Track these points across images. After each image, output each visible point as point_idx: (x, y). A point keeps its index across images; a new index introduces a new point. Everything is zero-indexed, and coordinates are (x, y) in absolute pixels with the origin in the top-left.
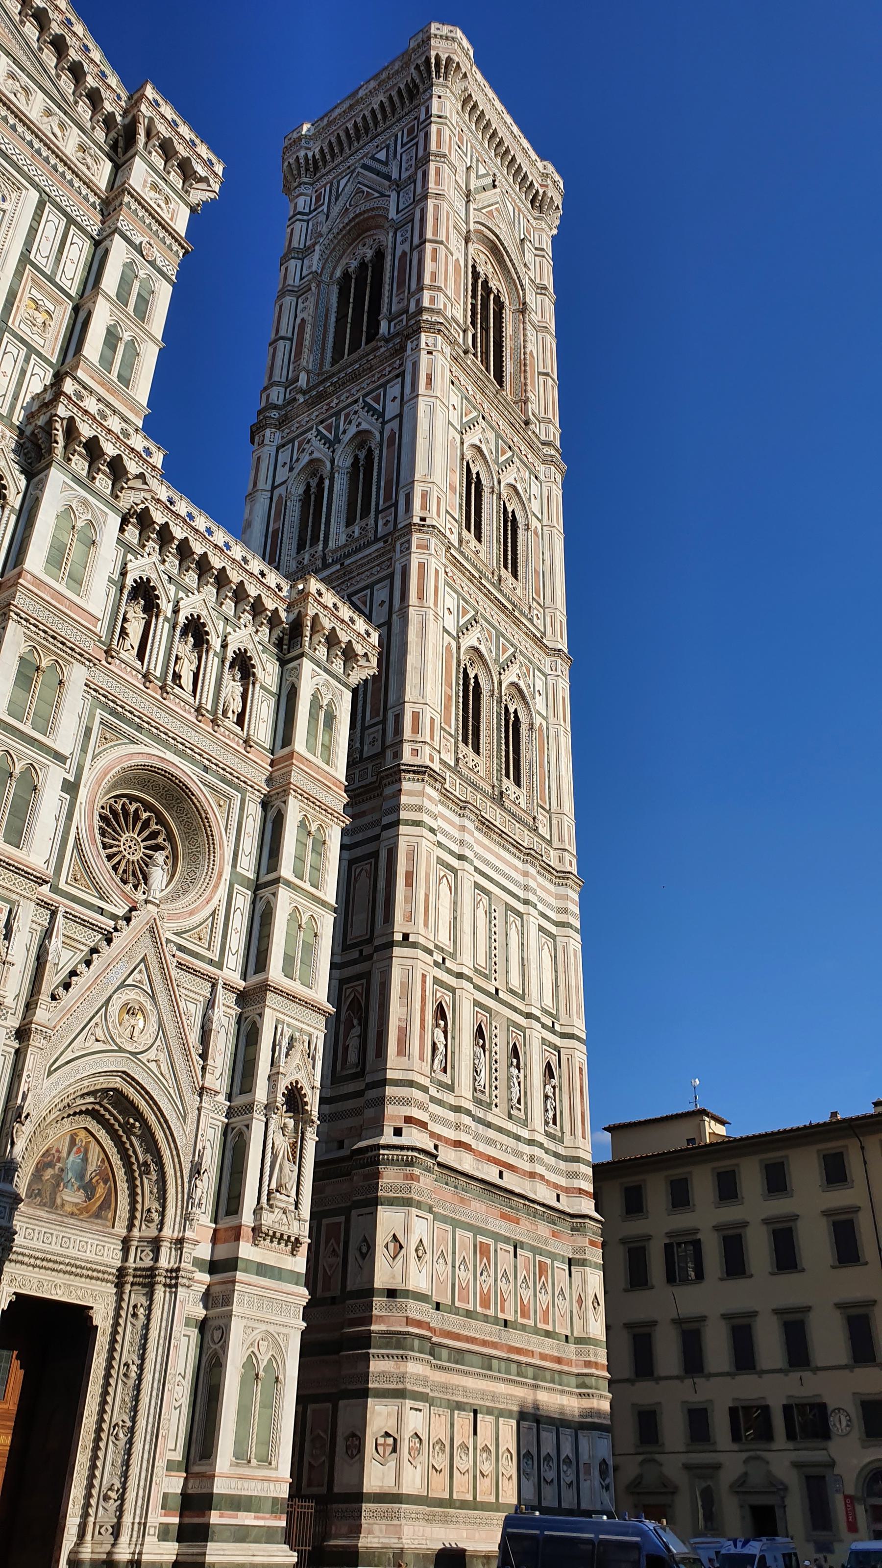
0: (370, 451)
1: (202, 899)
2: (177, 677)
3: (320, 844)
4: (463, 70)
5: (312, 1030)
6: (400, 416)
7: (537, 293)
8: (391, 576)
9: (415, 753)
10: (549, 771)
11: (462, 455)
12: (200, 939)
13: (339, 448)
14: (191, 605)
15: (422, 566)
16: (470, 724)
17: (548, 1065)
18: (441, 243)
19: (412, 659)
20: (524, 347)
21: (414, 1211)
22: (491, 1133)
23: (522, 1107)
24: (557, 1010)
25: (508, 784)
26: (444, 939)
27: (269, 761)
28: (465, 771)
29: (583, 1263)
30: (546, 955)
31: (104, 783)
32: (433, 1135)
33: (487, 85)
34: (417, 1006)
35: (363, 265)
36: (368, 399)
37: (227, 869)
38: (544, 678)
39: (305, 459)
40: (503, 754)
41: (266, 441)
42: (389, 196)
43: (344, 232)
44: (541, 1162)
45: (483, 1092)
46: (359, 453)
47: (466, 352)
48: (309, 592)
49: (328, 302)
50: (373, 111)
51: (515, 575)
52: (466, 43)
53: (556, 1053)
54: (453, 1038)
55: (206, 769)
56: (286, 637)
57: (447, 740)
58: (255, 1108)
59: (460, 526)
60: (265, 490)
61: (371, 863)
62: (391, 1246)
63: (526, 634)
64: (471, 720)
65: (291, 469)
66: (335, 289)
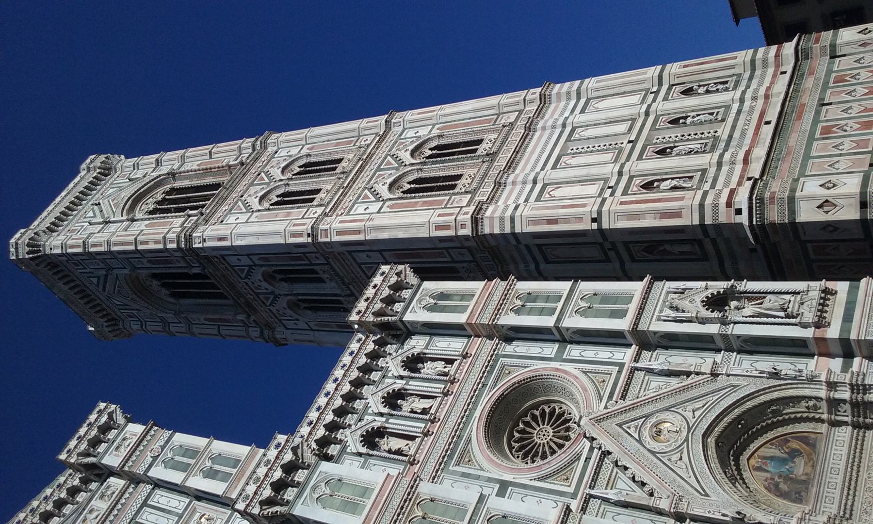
0: (275, 272)
1: (575, 383)
2: (425, 411)
3: (531, 297)
4: (33, 235)
5: (664, 291)
6: (248, 255)
8: (350, 252)
9: (463, 226)
10: (470, 119)
12: (604, 381)
13: (277, 292)
16: (442, 184)
17: (683, 93)
19: (401, 235)
20: (195, 171)
21: (798, 194)
22: (737, 134)
23: (716, 111)
24: (642, 90)
25: (482, 149)
26: (593, 189)
27: (476, 338)
28: (474, 186)
29: (833, 46)
31: (499, 462)
32: (740, 184)
33: (40, 217)
34: (643, 206)
35: (164, 285)
36: (243, 276)
38: (407, 130)
39: (289, 312)
40: (460, 156)
42: (117, 274)
43: (146, 299)
44: (756, 91)
45: (706, 144)
46: (278, 278)
47: (202, 214)
48: (359, 321)
51: (339, 161)
52: (17, 236)
53: (674, 87)
54: (666, 173)
55: (484, 385)
56: (391, 333)
57: (453, 201)
58: (724, 333)
59: (311, 206)
60: (314, 335)
61: (546, 249)
62: (826, 209)
63: (378, 148)
64: (439, 184)
65: (298, 320)
66: (182, 301)
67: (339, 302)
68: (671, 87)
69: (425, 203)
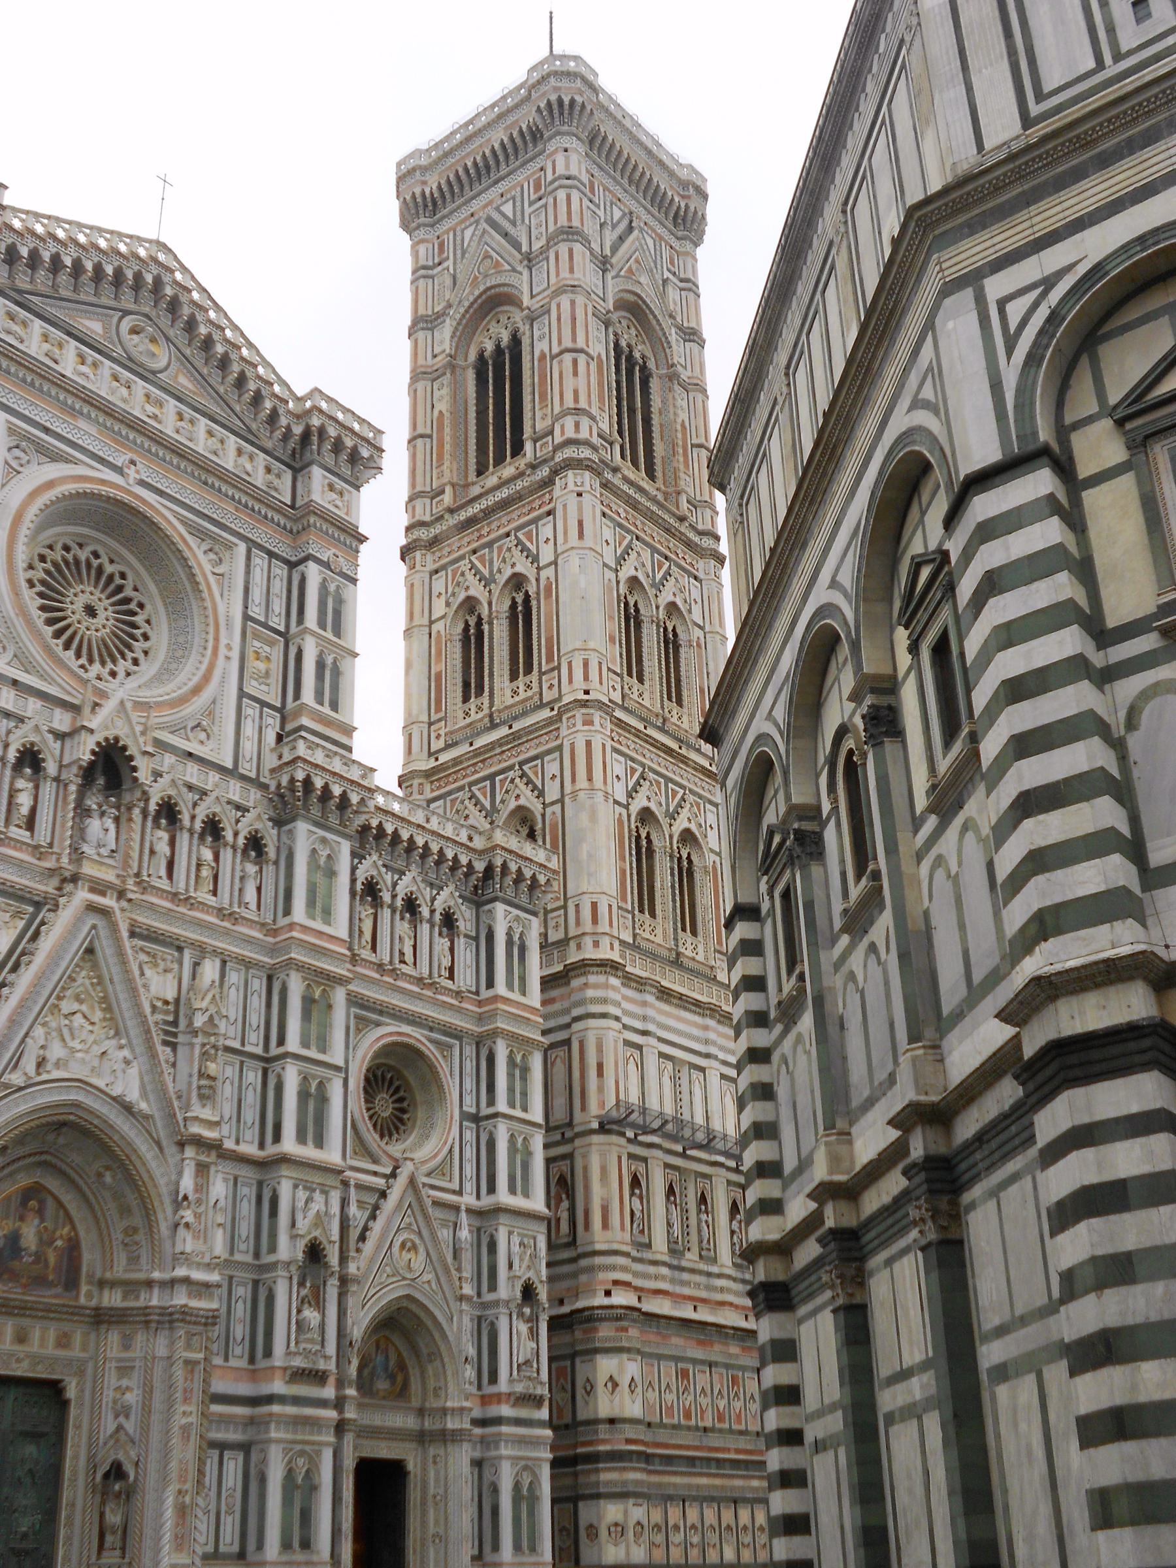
0: (527, 595)
3: (525, 1070)
6: (555, 563)
7: (685, 341)
8: (560, 748)
9: (596, 944)
11: (618, 596)
14: (405, 885)
15: (588, 744)
22: (686, 1276)
25: (686, 937)
28: (643, 944)
34: (616, 1185)
35: (499, 350)
36: (519, 534)
41: (418, 567)
50: (493, 151)
54: (648, 1202)
55: (431, 1029)
62: (610, 1385)
63: (695, 769)
65: (448, 604)
66: (471, 375)
69: (623, 872)
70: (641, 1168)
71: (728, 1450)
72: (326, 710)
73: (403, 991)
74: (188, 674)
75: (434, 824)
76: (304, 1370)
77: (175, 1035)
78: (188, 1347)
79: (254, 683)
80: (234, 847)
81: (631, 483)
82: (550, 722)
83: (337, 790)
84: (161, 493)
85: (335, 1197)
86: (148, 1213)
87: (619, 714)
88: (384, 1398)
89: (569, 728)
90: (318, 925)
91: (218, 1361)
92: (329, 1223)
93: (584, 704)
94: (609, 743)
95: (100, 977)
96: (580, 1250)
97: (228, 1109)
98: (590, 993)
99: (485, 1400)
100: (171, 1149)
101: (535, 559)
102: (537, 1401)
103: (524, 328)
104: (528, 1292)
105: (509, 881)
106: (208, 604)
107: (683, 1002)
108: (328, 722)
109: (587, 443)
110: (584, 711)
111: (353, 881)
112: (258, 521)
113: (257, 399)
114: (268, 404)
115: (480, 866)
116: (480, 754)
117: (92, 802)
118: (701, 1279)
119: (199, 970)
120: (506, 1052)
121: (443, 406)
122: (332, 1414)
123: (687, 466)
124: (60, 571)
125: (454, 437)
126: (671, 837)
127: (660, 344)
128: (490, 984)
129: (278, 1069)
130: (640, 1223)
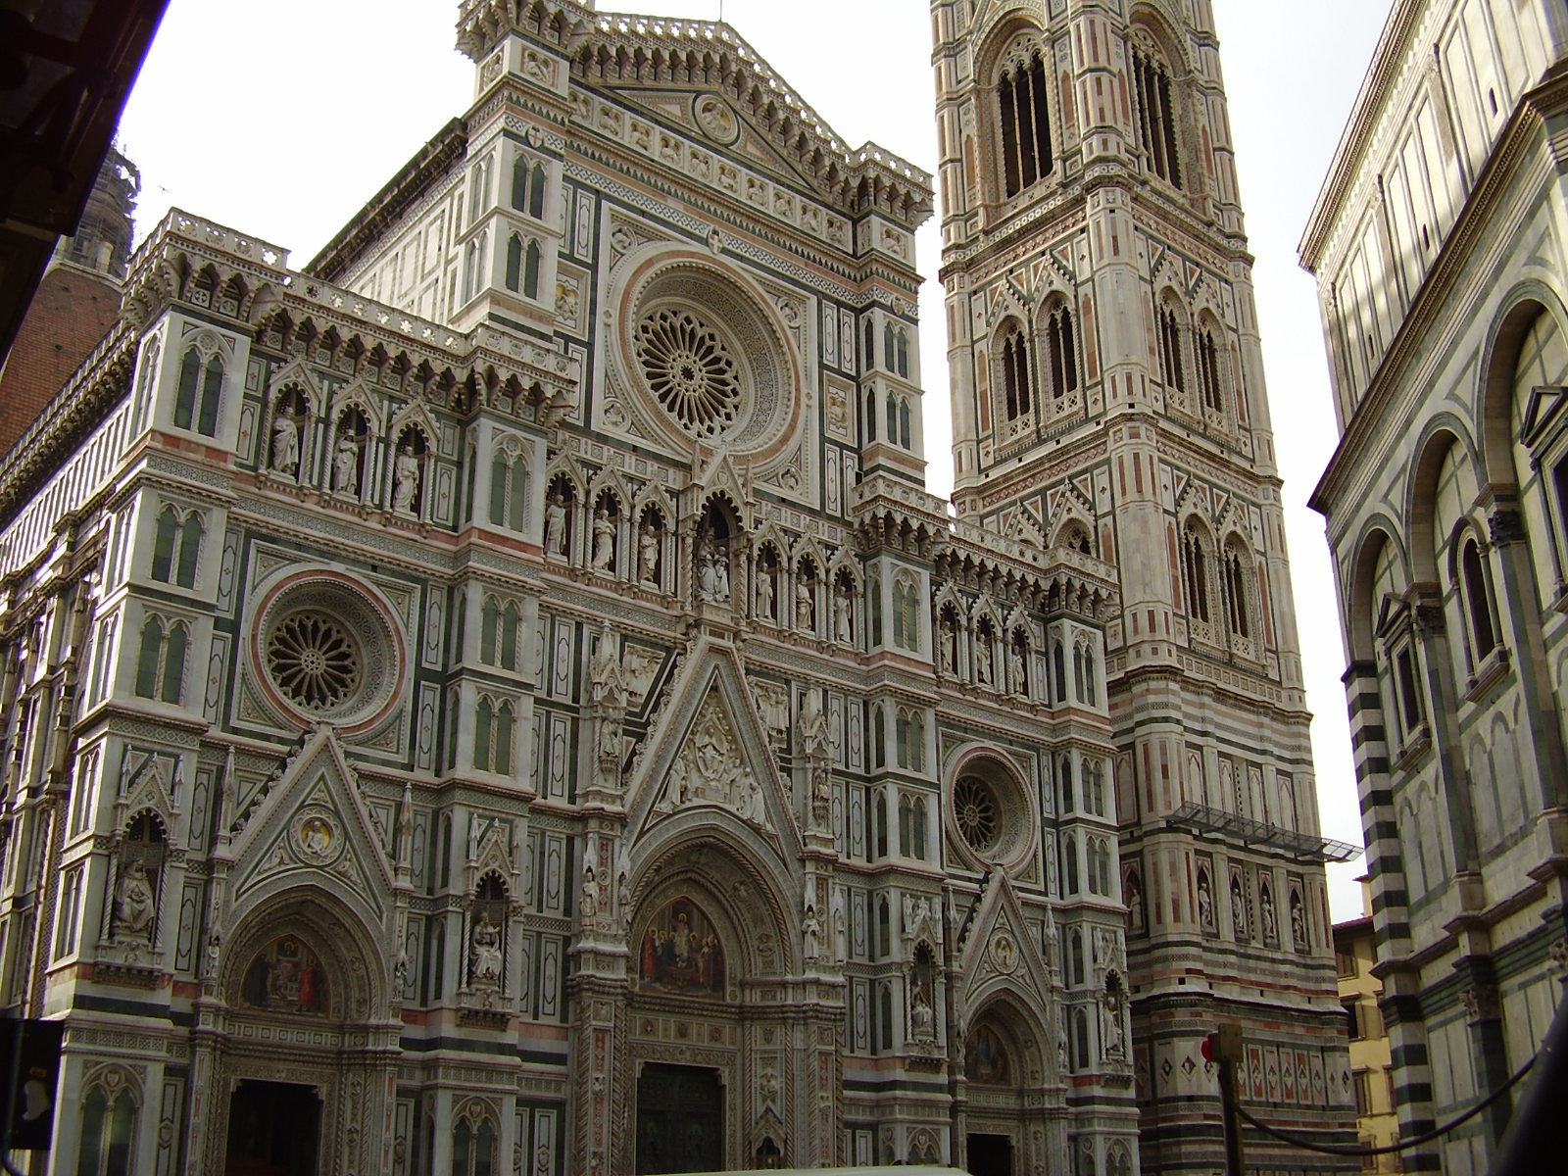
0: (1066, 312)
3: (1099, 776)
8: (1108, 461)
9: (1155, 651)
15: (1136, 456)
18: (1104, 69)
22: (1252, 963)
25: (1237, 637)
28: (1199, 648)
30: (1285, 794)
37: (1038, 818)
49: (991, 113)
55: (1011, 743)
63: (1237, 472)
65: (988, 324)
66: (995, 98)
67: (1025, 409)
68: (1301, 876)
69: (1175, 579)
70: (1207, 863)
71: (1296, 1123)
72: (899, 447)
73: (984, 708)
74: (775, 428)
75: (988, 544)
76: (921, 1059)
77: (789, 761)
78: (821, 1040)
79: (833, 427)
80: (827, 585)
81: (1160, 194)
82: (1096, 436)
83: (915, 524)
84: (741, 258)
85: (937, 902)
86: (779, 924)
87: (1163, 424)
88: (986, 1082)
89: (1116, 441)
90: (906, 652)
91: (846, 1052)
92: (935, 927)
93: (1129, 418)
94: (1156, 455)
95: (724, 712)
96: (1154, 941)
97: (839, 826)
98: (1152, 699)
99: (1078, 1082)
100: (794, 865)
101: (1073, 277)
102: (1125, 1082)
103: (1045, 49)
104: (1112, 982)
105: (1074, 596)
106: (789, 357)
107: (1238, 702)
108: (902, 460)
109: (1115, 160)
110: (1130, 424)
111: (933, 607)
112: (826, 274)
113: (817, 157)
114: (827, 162)
115: (1046, 585)
116: (1029, 470)
117: (705, 553)
118: (1267, 965)
119: (806, 700)
120: (1081, 761)
121: (972, 130)
122: (949, 1097)
123: (1211, 172)
124: (659, 339)
125: (983, 160)
126: (1218, 541)
127: (1177, 52)
128: (1062, 697)
129: (880, 788)
130: (1210, 914)
